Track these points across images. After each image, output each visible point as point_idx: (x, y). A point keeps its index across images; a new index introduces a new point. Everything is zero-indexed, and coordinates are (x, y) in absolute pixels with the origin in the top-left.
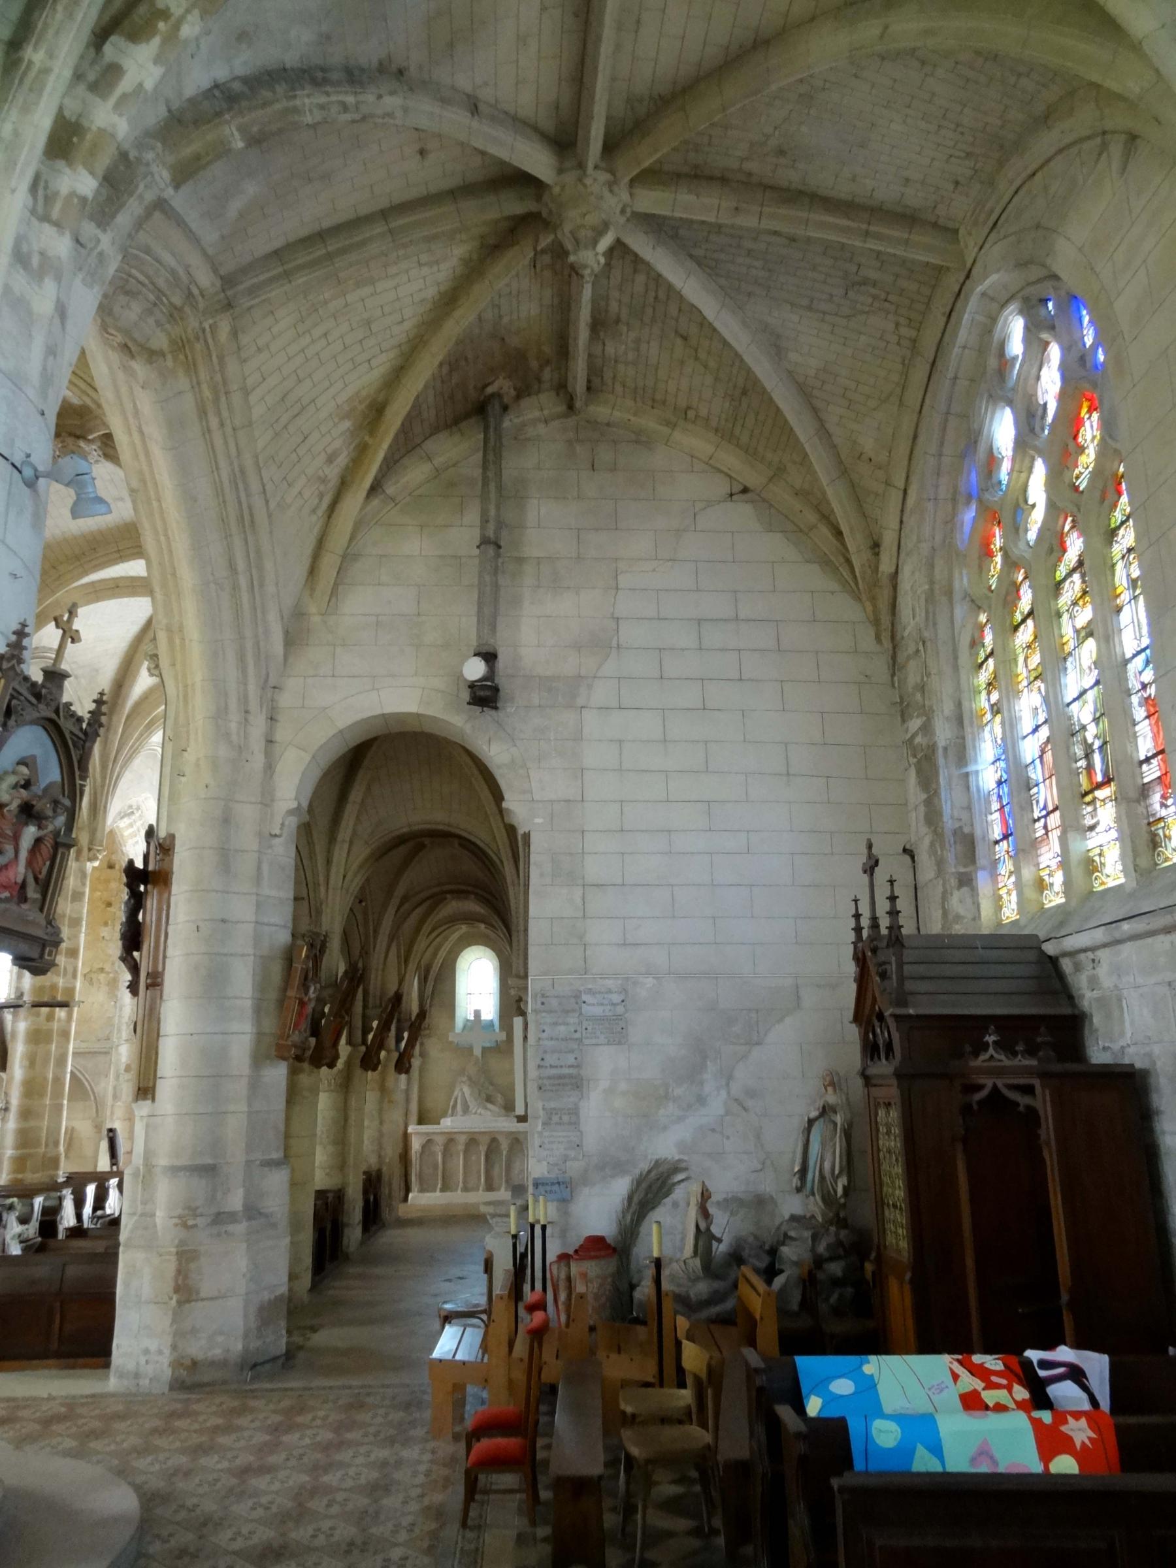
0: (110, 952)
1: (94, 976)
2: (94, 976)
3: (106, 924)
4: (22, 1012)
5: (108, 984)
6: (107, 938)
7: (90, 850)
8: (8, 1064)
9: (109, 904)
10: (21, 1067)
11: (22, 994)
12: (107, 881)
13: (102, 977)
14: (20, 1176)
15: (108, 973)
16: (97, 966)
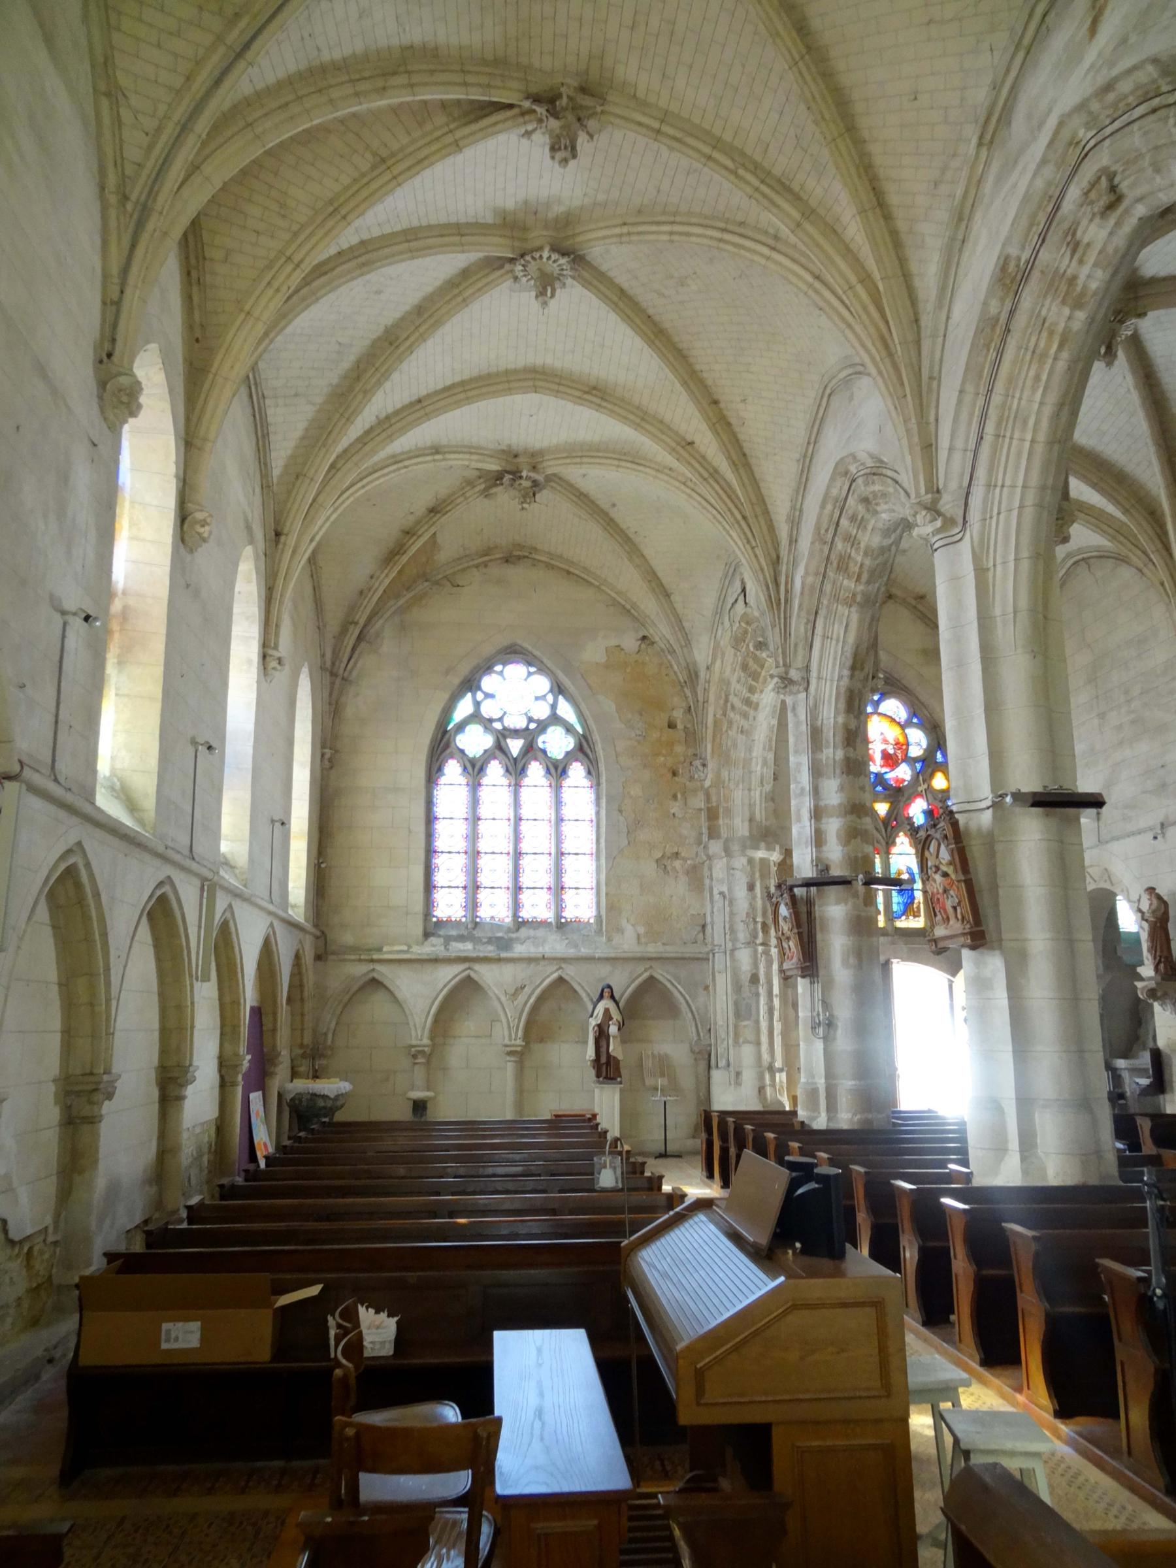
0: (685, 832)
1: (668, 863)
2: (668, 863)
3: (675, 797)
4: (832, 892)
5: (688, 873)
6: (679, 814)
7: (873, 677)
8: (821, 963)
9: (674, 774)
10: (845, 963)
11: (827, 868)
12: (671, 744)
13: (677, 864)
14: (870, 1116)
15: (685, 860)
16: (670, 850)
